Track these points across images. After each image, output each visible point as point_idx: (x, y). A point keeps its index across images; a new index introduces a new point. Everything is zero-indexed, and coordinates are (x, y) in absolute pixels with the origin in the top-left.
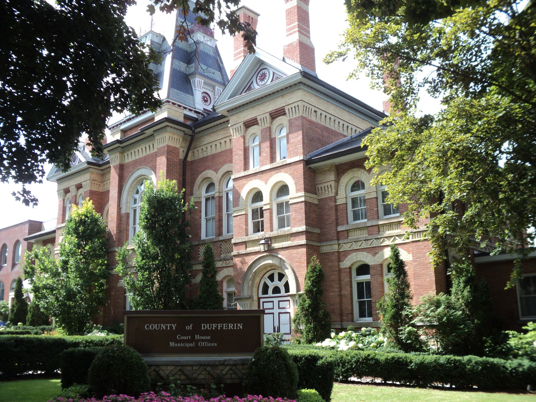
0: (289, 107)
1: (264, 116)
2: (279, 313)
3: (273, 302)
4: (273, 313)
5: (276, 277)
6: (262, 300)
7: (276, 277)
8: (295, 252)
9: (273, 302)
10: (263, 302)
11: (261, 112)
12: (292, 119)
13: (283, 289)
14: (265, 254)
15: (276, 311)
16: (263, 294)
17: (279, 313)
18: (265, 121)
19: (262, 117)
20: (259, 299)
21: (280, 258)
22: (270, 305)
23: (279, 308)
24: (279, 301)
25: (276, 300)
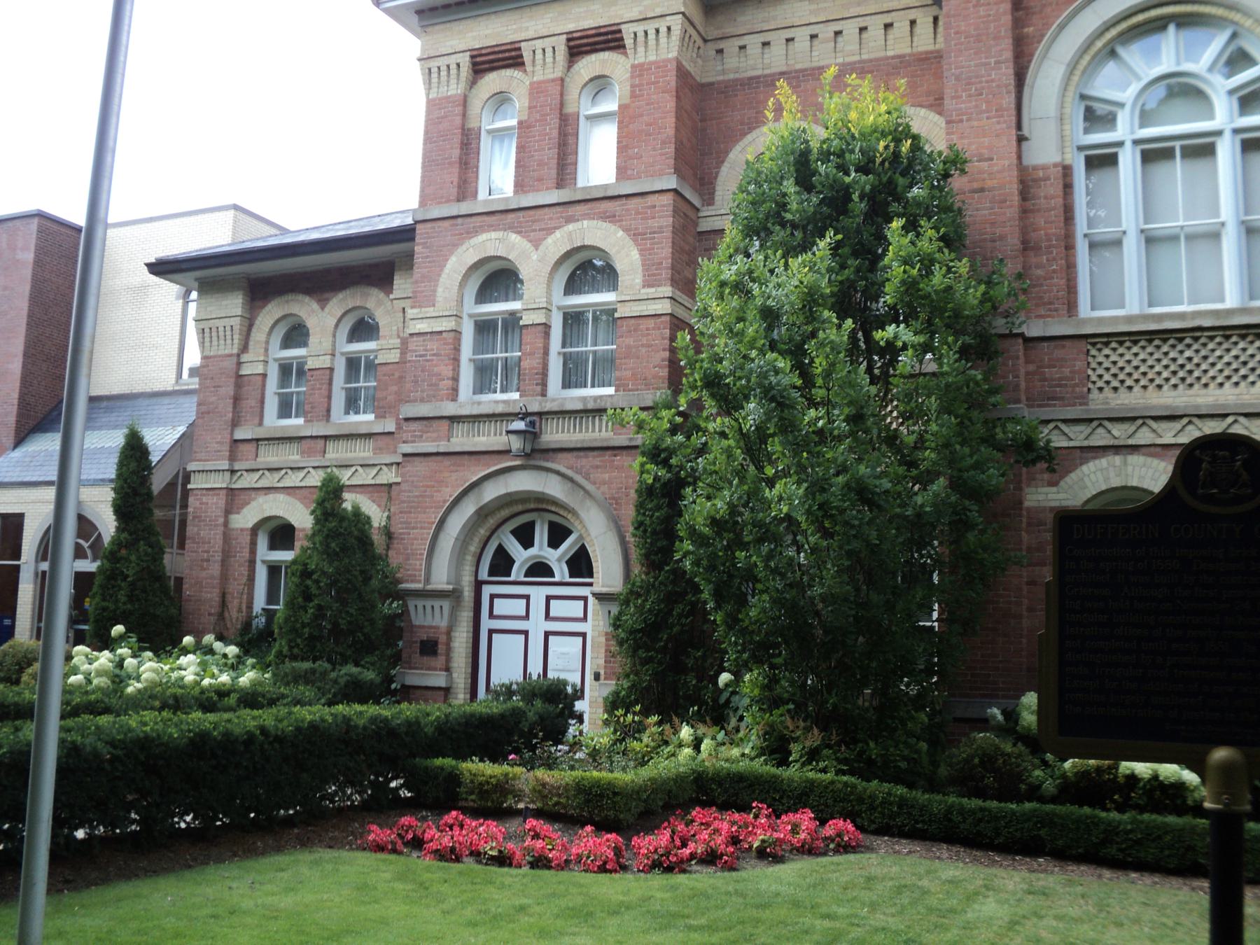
3: (527, 597)
4: (526, 633)
6: (487, 590)
9: (527, 597)
10: (493, 597)
15: (537, 626)
16: (492, 573)
17: (547, 635)
20: (478, 585)
23: (547, 616)
24: (549, 598)
25: (538, 594)
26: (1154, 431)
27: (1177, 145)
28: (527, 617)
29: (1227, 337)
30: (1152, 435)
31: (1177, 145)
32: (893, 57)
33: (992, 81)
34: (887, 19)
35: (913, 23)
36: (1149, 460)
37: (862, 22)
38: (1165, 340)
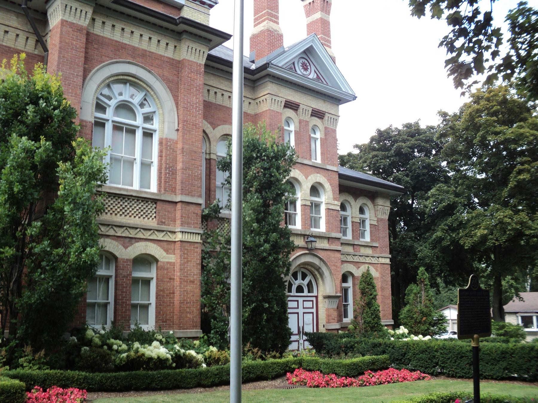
0: (330, 116)
1: (308, 108)
2: (304, 313)
3: (298, 301)
4: (298, 313)
5: (299, 276)
7: (299, 276)
8: (333, 256)
9: (298, 301)
11: (308, 103)
12: (329, 128)
13: (306, 290)
14: (307, 252)
18: (307, 114)
19: (305, 107)
21: (321, 259)
22: (294, 304)
25: (301, 300)
26: (115, 230)
27: (125, 127)
28: (298, 308)
29: (138, 200)
30: (128, 233)
31: (125, 127)
32: (6, 46)
33: (75, 82)
34: (7, 29)
35: (17, 35)
36: (112, 241)
37: (7, 29)
38: (119, 198)
